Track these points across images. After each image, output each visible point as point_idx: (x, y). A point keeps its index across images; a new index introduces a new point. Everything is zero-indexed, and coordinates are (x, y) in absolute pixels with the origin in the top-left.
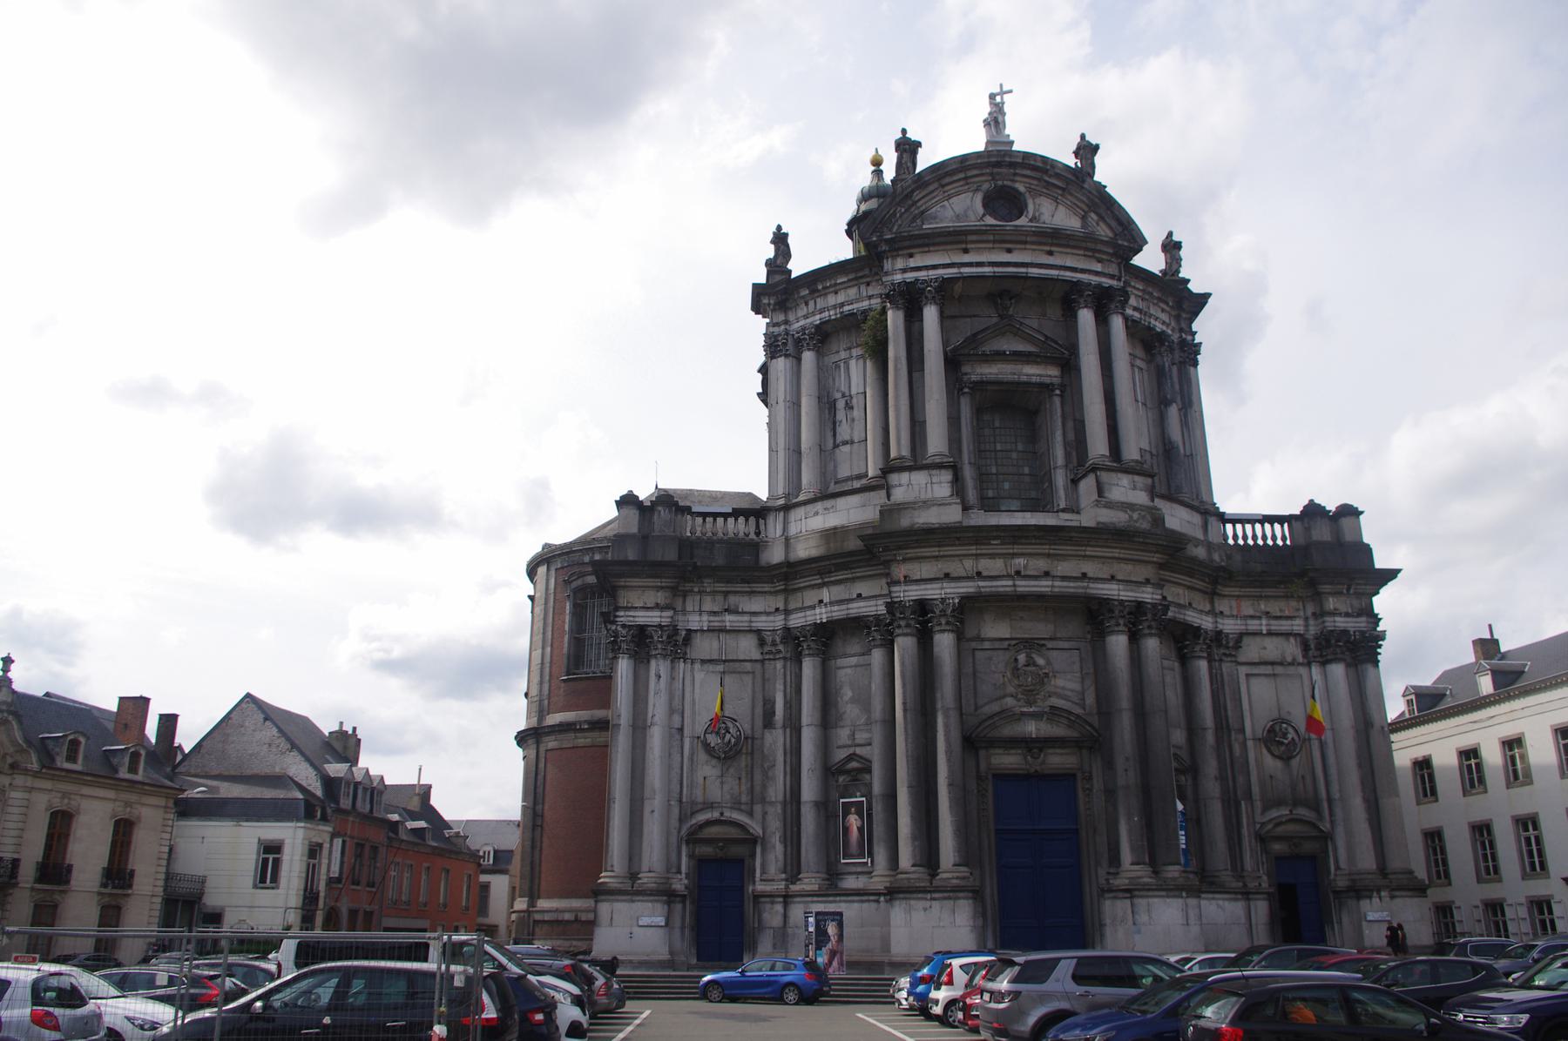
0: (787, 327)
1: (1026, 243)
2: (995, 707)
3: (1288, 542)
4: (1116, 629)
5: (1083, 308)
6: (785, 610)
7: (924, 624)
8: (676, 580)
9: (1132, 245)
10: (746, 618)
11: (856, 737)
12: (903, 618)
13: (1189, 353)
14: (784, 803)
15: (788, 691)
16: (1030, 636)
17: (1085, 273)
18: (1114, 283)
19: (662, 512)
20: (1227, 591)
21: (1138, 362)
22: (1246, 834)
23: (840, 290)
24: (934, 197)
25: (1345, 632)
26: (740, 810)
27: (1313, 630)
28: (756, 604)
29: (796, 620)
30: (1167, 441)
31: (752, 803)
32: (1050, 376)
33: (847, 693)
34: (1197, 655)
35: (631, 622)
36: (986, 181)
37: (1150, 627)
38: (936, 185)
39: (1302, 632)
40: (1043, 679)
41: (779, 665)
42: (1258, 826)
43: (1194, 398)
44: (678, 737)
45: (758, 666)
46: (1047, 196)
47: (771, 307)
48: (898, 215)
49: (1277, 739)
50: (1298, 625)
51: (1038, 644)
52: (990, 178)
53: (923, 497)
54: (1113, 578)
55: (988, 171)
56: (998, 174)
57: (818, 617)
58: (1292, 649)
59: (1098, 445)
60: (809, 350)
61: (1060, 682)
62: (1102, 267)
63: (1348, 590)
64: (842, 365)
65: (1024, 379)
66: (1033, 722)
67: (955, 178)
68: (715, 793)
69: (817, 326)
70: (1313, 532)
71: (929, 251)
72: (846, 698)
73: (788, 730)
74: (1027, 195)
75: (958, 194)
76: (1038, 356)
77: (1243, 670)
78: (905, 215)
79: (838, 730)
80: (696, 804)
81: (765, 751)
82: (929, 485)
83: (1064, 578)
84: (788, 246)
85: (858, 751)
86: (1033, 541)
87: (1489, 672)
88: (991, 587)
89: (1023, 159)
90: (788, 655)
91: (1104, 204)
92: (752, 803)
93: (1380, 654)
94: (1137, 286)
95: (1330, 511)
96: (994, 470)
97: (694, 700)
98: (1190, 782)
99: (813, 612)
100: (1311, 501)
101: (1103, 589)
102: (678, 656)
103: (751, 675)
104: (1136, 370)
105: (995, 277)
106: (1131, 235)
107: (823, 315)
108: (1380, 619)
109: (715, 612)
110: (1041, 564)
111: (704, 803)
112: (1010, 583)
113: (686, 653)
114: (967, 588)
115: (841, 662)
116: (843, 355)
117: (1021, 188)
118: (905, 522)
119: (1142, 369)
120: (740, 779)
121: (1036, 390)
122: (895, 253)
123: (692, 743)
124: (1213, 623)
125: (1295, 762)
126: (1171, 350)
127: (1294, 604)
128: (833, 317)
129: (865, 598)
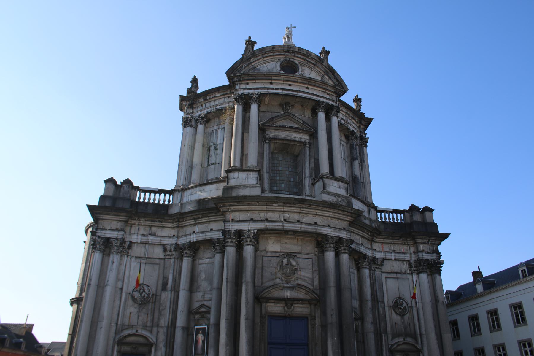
0: (193, 115)
1: (297, 82)
2: (271, 283)
3: (403, 222)
4: (329, 249)
5: (320, 111)
6: (177, 236)
7: (240, 242)
8: (127, 218)
9: (342, 90)
10: (159, 238)
11: (205, 297)
12: (230, 238)
13: (364, 141)
14: (168, 327)
15: (175, 273)
16: (290, 251)
17: (322, 98)
18: (334, 104)
19: (125, 187)
20: (377, 240)
21: (342, 143)
22: (385, 349)
23: (216, 100)
24: (260, 62)
25: (427, 260)
26: (146, 330)
27: (414, 258)
28: (165, 232)
29: (182, 241)
30: (354, 175)
31: (152, 327)
32: (305, 139)
33: (203, 276)
34: (365, 267)
35: (103, 235)
36: (282, 58)
37: (345, 249)
38: (261, 57)
39: (409, 260)
40: (294, 271)
41: (172, 261)
42: (390, 346)
43: (365, 159)
44: (119, 292)
45: (162, 261)
46: (308, 67)
47: (187, 106)
48: (244, 67)
49: (398, 306)
50: (407, 257)
51: (293, 255)
52: (284, 57)
53: (244, 184)
54: (329, 226)
55: (283, 53)
56: (287, 55)
57: (192, 239)
58: (405, 267)
59: (325, 168)
60: (201, 124)
61: (302, 273)
62: (329, 97)
63: (428, 242)
64: (215, 132)
65: (293, 139)
66: (289, 291)
67: (269, 55)
68: (134, 321)
69: (205, 114)
70: (414, 217)
71: (255, 82)
72: (202, 278)
73: (173, 292)
74: (299, 65)
75: (270, 62)
76: (300, 129)
77: (384, 275)
78: (247, 68)
79: (197, 293)
80: (125, 325)
81: (161, 301)
82: (247, 179)
83: (306, 224)
84: (197, 84)
85: (206, 303)
86: (293, 206)
87: (482, 283)
88: (272, 226)
89: (298, 50)
90: (176, 257)
91: (331, 72)
92: (152, 327)
93: (441, 270)
94: (343, 110)
95: (421, 209)
96: (278, 178)
97: (129, 276)
98: (360, 324)
99: (189, 237)
100: (413, 205)
101: (324, 230)
102: (124, 254)
103: (158, 265)
104: (342, 145)
105: (283, 95)
106: (342, 86)
107: (208, 110)
108: (441, 256)
109: (144, 235)
110: (296, 217)
111: (129, 325)
112: (281, 224)
113: (128, 253)
114: (261, 225)
115: (201, 261)
116: (216, 127)
117: (297, 62)
118: (234, 194)
119: (344, 145)
120: (147, 314)
121: (298, 144)
122: (241, 82)
123: (126, 296)
124: (371, 254)
125: (406, 317)
126: (356, 138)
127: (405, 247)
128: (212, 111)
129: (214, 231)
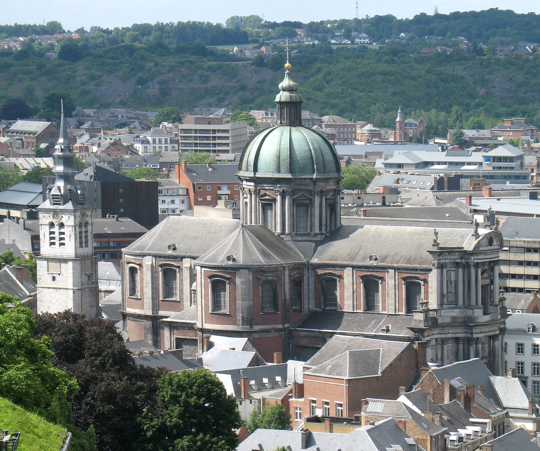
29: (443, 336)
